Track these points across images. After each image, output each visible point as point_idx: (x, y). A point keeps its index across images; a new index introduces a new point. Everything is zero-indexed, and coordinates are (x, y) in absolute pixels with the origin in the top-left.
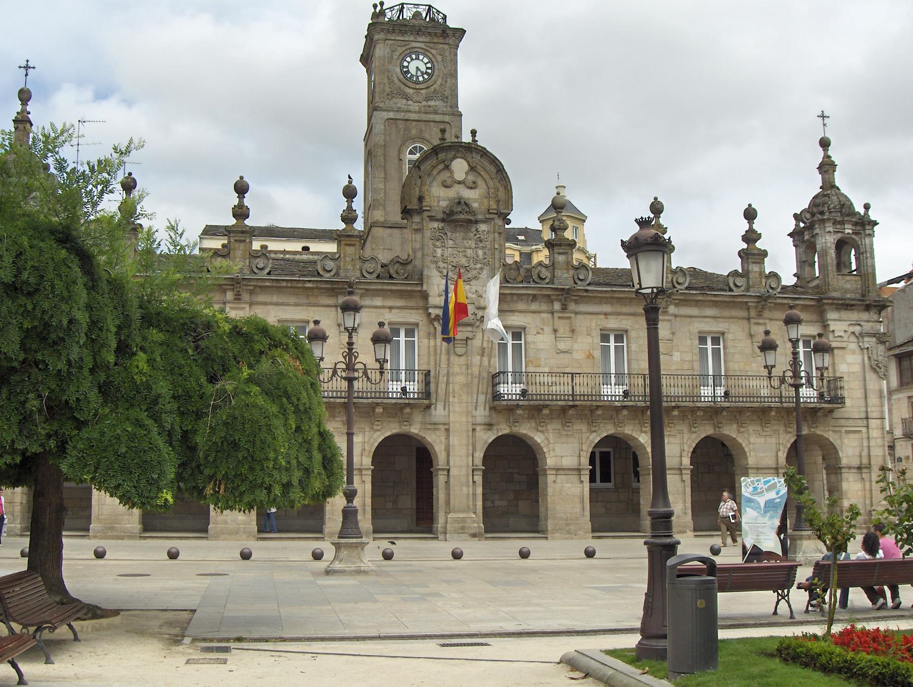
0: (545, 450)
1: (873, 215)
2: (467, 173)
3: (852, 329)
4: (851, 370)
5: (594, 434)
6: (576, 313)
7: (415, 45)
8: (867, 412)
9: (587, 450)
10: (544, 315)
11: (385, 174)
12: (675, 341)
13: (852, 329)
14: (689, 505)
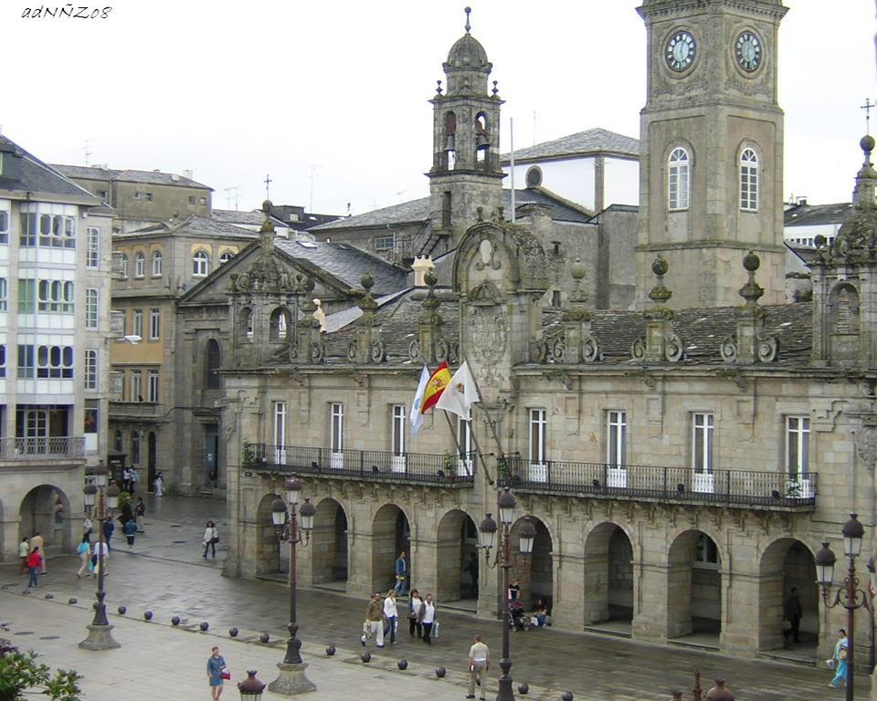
2: (492, 255)
3: (838, 407)
7: (678, 22)
11: (649, 189)
13: (838, 407)
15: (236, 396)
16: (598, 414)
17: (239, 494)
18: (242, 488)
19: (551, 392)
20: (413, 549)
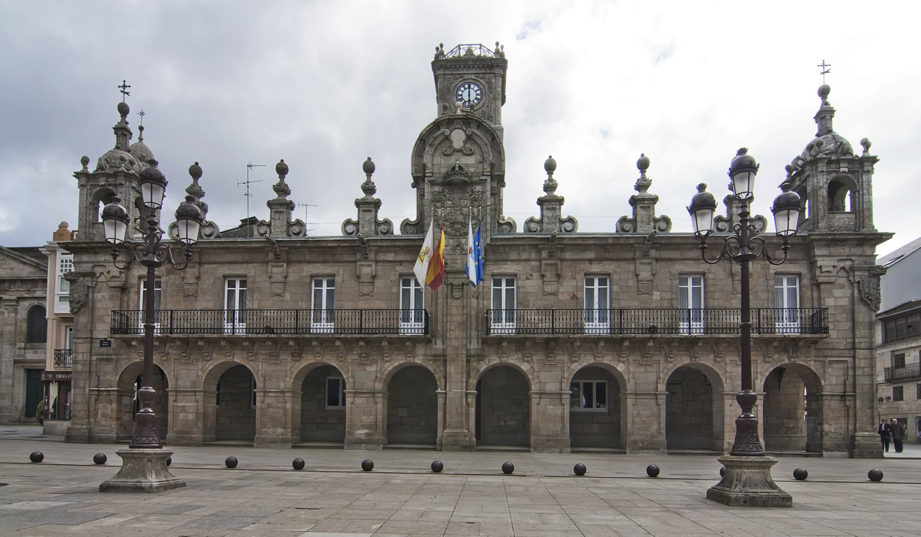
0: (530, 377)
1: (872, 152)
3: (841, 264)
4: (839, 304)
5: (576, 364)
6: (562, 260)
8: (854, 343)
9: (568, 376)
10: (533, 263)
12: (655, 282)
13: (841, 264)
14: (663, 425)
15: (90, 270)
16: (580, 277)
17: (90, 364)
18: (94, 358)
19: (525, 260)
20: (348, 400)
